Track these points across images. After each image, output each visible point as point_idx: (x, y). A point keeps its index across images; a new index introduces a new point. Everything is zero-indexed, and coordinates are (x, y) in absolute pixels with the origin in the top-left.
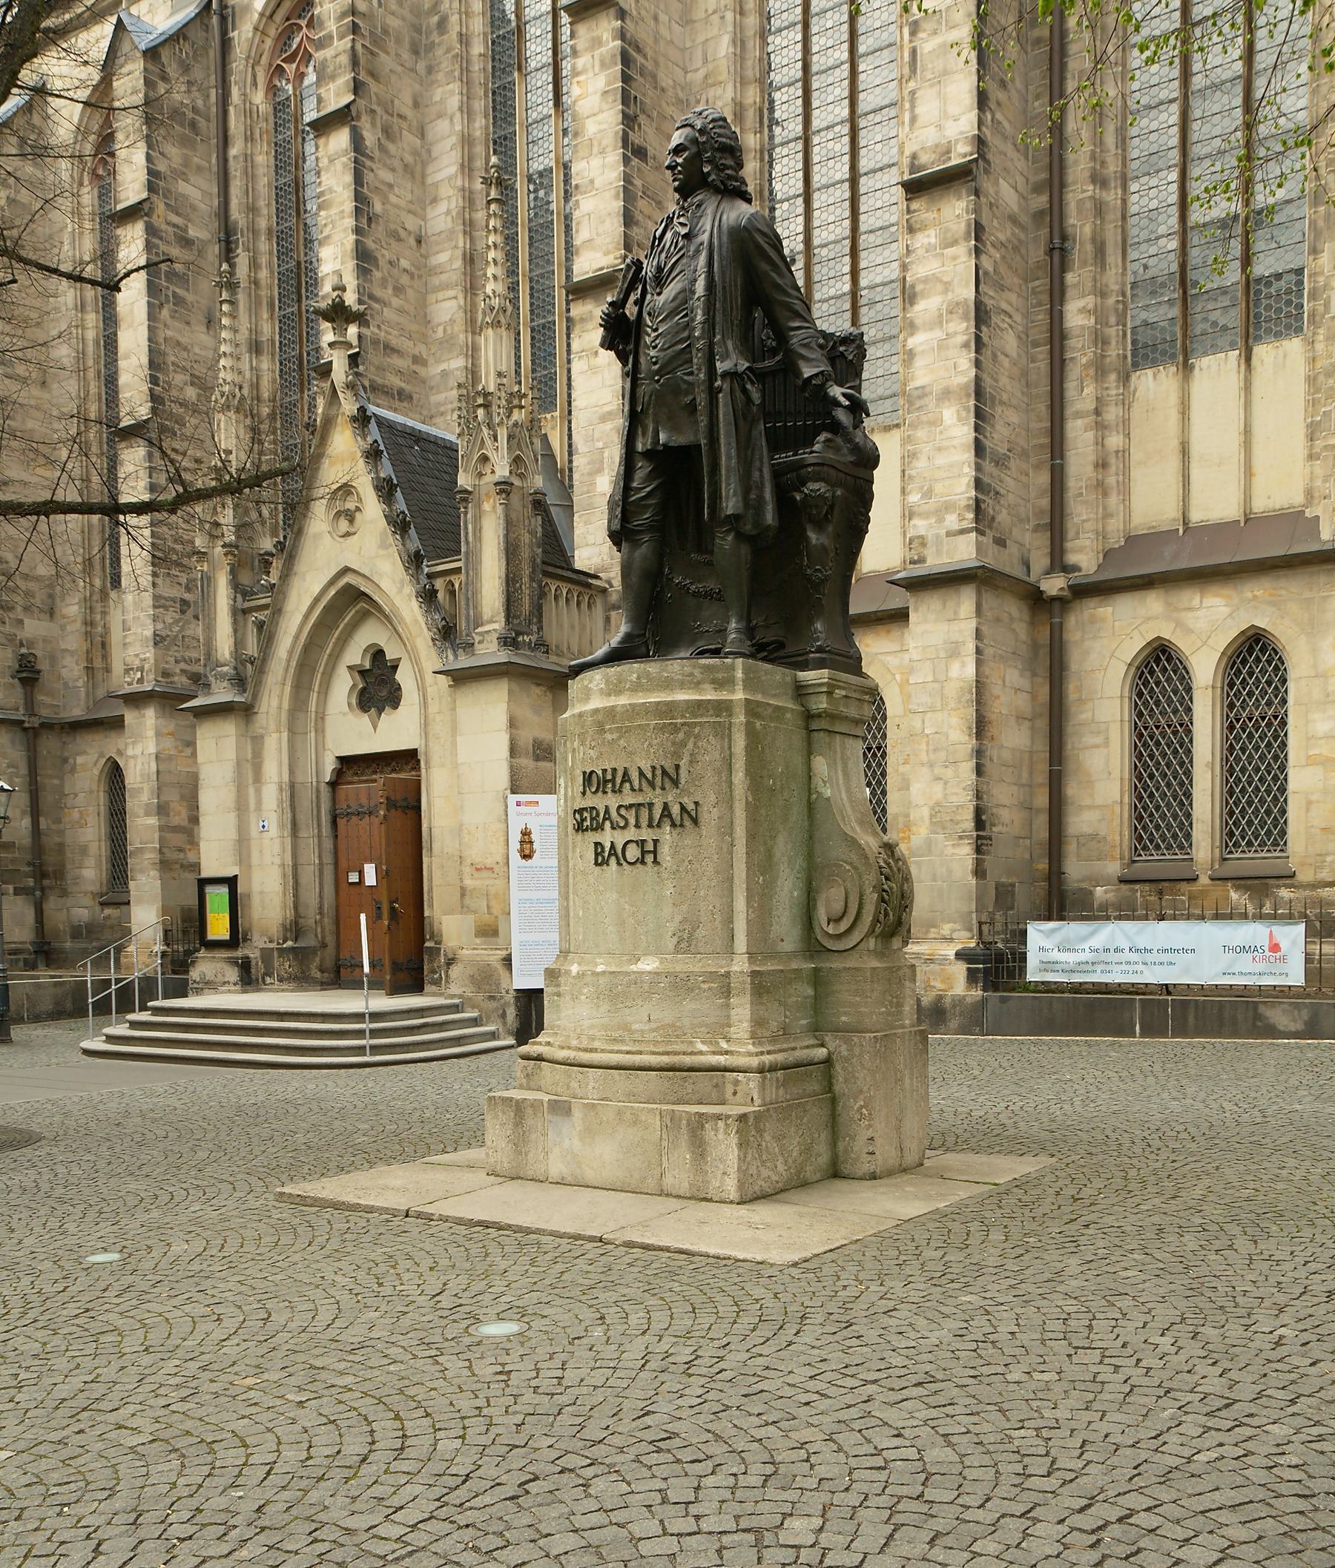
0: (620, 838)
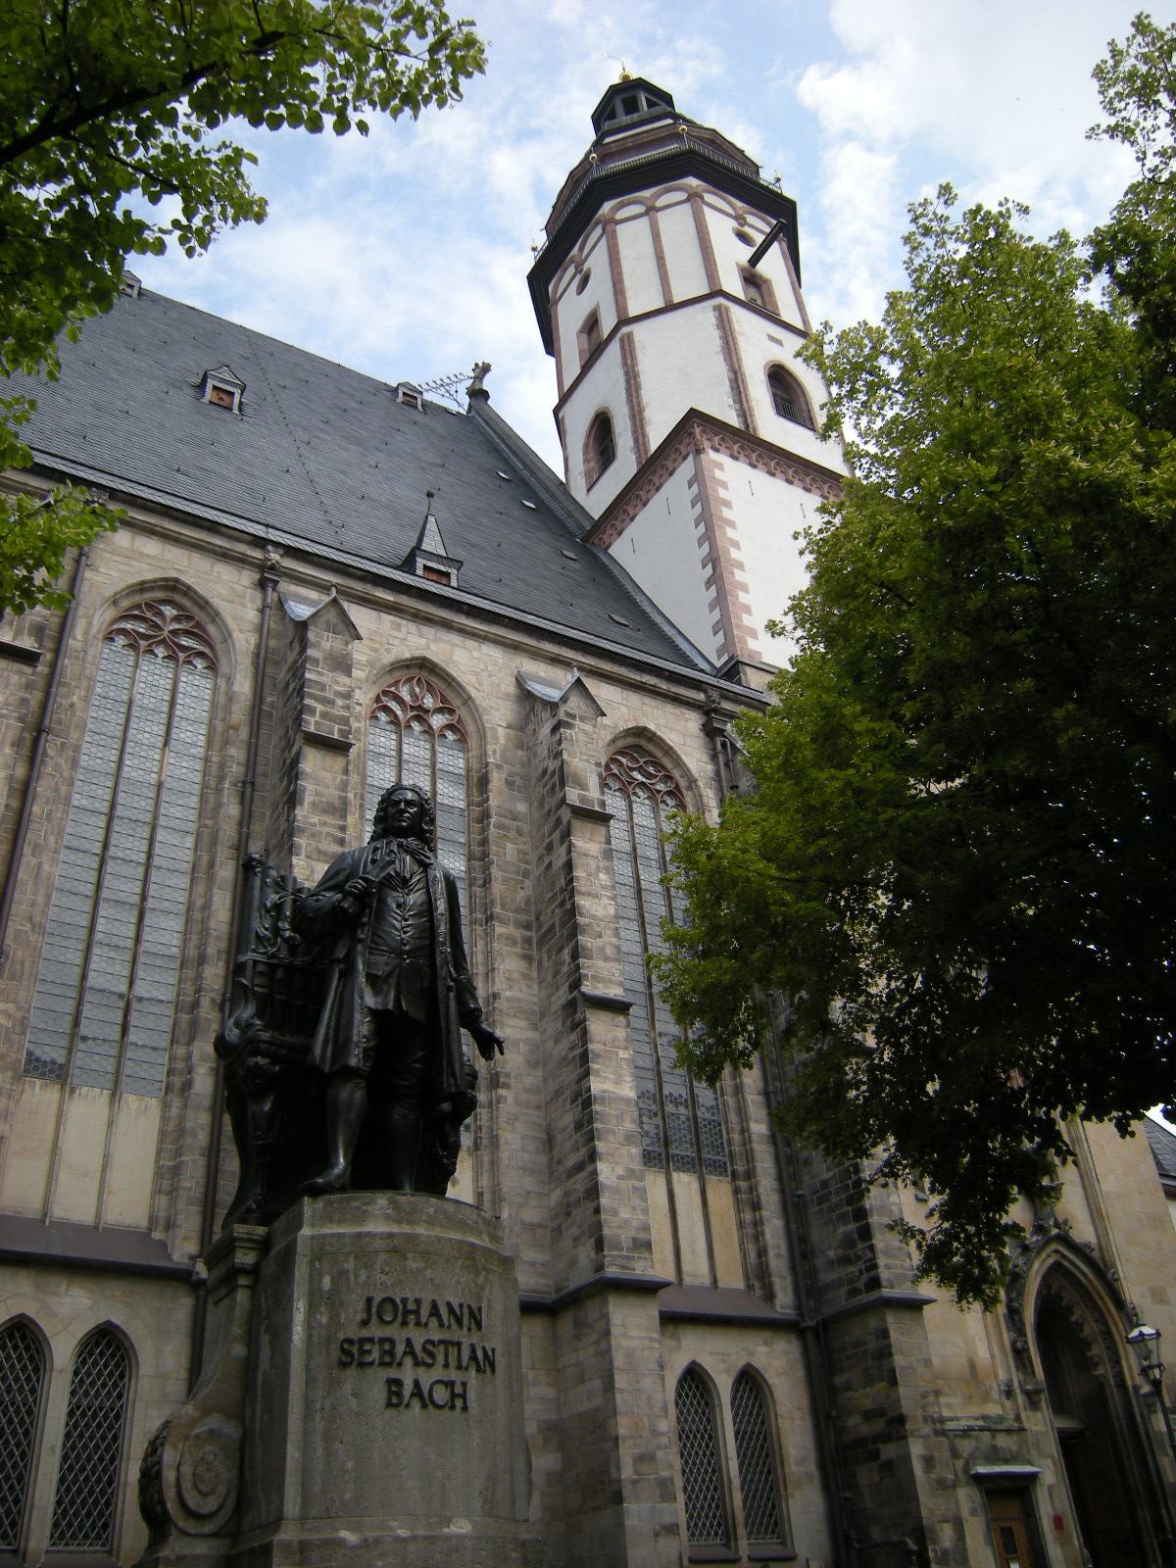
0: (427, 1378)
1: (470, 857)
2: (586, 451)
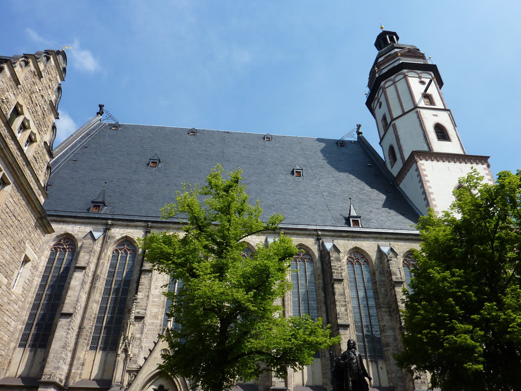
1: (374, 293)
2: (389, 155)
